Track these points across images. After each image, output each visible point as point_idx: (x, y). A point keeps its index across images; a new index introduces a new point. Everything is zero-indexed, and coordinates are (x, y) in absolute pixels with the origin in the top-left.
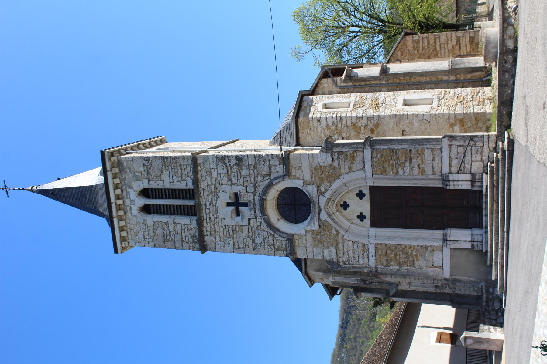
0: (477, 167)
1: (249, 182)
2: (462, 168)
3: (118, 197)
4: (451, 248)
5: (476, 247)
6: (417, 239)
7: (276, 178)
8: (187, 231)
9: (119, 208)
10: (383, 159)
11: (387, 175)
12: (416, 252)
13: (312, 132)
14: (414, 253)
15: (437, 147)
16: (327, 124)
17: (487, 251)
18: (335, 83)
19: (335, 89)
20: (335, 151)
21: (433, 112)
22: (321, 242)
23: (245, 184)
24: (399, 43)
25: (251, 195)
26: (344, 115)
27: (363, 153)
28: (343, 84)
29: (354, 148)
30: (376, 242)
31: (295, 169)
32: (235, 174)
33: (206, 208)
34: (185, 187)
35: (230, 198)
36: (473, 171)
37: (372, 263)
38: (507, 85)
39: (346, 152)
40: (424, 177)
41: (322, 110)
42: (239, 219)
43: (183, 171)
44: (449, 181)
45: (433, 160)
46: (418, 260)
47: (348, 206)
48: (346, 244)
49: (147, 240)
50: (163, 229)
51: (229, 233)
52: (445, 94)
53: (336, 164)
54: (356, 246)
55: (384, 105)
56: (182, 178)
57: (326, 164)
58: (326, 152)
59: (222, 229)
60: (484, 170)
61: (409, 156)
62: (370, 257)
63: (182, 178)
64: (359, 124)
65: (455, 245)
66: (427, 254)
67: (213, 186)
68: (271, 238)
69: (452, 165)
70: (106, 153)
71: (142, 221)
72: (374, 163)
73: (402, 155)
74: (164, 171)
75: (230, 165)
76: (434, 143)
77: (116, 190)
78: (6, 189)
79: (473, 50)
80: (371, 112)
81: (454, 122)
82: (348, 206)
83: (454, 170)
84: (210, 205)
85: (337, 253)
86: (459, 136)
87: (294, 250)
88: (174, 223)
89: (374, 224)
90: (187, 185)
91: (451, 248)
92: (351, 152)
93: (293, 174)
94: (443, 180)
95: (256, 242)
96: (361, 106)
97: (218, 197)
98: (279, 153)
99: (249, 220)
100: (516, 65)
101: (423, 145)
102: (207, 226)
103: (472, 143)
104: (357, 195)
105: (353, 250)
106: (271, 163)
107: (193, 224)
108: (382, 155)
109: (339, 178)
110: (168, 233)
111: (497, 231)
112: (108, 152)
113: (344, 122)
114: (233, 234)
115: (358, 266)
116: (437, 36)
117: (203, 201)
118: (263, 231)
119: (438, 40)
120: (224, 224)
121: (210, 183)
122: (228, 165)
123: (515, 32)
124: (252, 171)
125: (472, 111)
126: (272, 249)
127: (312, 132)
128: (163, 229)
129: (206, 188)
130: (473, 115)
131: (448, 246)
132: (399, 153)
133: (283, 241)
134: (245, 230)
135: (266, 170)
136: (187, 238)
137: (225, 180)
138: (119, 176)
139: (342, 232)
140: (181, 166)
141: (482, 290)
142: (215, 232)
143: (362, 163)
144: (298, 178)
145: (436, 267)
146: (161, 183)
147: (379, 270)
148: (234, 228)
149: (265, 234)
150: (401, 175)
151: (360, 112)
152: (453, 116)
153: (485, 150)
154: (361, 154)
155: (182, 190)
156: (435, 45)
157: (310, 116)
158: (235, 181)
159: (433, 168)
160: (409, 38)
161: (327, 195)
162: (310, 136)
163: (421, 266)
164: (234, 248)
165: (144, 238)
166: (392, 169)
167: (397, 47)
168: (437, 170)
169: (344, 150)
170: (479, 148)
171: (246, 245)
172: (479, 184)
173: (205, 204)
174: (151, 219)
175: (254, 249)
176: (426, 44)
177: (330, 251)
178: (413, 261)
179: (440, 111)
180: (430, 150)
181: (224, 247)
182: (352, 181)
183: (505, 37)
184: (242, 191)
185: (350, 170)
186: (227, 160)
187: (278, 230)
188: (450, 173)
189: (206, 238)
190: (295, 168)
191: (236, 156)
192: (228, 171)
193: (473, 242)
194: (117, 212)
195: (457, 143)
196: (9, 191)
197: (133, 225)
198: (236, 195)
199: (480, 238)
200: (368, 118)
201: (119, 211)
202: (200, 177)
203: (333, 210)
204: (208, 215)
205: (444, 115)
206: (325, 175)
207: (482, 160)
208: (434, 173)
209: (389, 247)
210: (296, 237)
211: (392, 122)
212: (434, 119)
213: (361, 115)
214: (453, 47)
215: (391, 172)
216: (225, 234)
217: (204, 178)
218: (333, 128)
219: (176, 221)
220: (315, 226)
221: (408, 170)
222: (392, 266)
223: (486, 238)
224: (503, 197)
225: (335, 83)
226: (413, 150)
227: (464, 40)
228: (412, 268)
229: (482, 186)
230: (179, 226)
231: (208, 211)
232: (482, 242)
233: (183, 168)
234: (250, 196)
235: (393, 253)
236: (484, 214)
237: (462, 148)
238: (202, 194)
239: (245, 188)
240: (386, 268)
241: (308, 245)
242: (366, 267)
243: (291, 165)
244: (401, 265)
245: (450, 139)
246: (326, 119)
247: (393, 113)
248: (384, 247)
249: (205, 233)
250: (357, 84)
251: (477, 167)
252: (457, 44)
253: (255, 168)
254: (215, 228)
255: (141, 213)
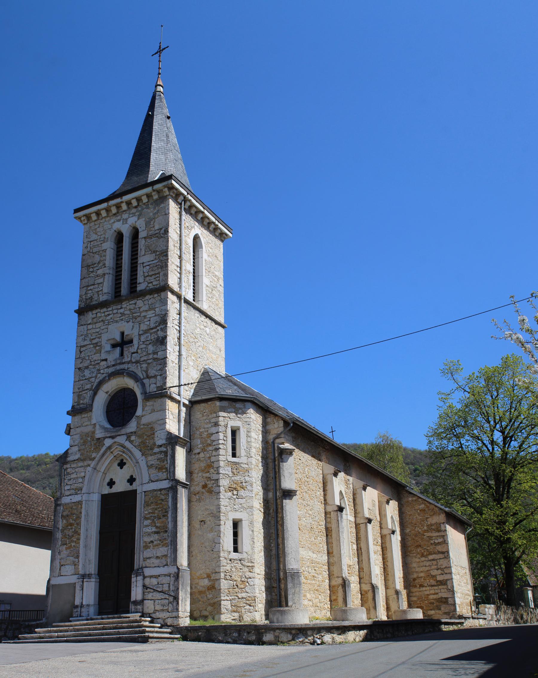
0: (149, 607)
1: (141, 355)
2: (149, 590)
3: (129, 203)
4: (75, 583)
5: (75, 610)
6: (86, 546)
7: (143, 385)
8: (97, 290)
9: (118, 206)
10: (159, 502)
11: (144, 507)
12: (74, 546)
13: (205, 418)
14: (73, 544)
15: (169, 560)
16: (212, 434)
17: (71, 621)
18: (278, 437)
19: (271, 437)
20: (168, 448)
21: (222, 554)
22: (85, 443)
23: (139, 351)
24: (436, 506)
25: (129, 359)
26: (222, 452)
27: (165, 480)
28: (276, 445)
29: (170, 469)
30: (84, 502)
31: (153, 405)
32: (150, 337)
33: (118, 309)
34: (138, 282)
35: (127, 335)
36: (145, 602)
37: (65, 500)
38: (226, 635)
39: (167, 460)
40: (142, 549)
41: (229, 426)
42: (108, 347)
43: (153, 277)
44: (136, 576)
45: (157, 557)
46: (66, 549)
47: (121, 468)
48: (82, 468)
49: (89, 245)
50: (99, 263)
51: (95, 339)
52: (248, 567)
53: (156, 450)
54: (80, 480)
55: (235, 497)
56: (147, 276)
57: (156, 439)
58: (167, 438)
59: (98, 330)
60: (146, 614)
61: (161, 530)
62: (70, 497)
63: (147, 276)
64: (212, 470)
65: (78, 588)
66: (72, 558)
67: (139, 314)
68: (89, 386)
69: (152, 579)
70: (169, 182)
71: (106, 237)
72: (155, 493)
73: (162, 522)
74: (154, 254)
75: (158, 330)
76: (173, 557)
77: (135, 200)
78: (160, 51)
79: (431, 603)
80: (224, 483)
81: (212, 578)
82: (121, 468)
83: (147, 581)
84: (121, 313)
85: (75, 460)
86: (178, 584)
87: (78, 413)
88: (104, 274)
89: (105, 498)
90: (140, 283)
91: (75, 583)
92: (166, 466)
93: (148, 404)
94: (138, 570)
95: (86, 371)
96: (234, 471)
97: (128, 322)
98: (168, 385)
99: (106, 360)
100: (245, 644)
101: (171, 545)
102: (101, 313)
103: (171, 599)
104: (132, 476)
105: (77, 478)
106: (159, 377)
107: (103, 297)
108: (162, 500)
109: (142, 455)
110: (95, 269)
111: (78, 630)
112: (172, 184)
113: (214, 453)
114: (93, 344)
115: (63, 485)
116: (446, 554)
117: (124, 305)
118: (96, 377)
119: (441, 556)
120: (102, 332)
121: (141, 310)
122: (158, 328)
123: (283, 643)
124: (151, 356)
125: (222, 598)
126: (79, 389)
127: (205, 418)
128: (99, 263)
129: (137, 307)
130: (219, 599)
131: (78, 581)
132: (164, 519)
133: (87, 400)
134: (96, 357)
135: (152, 372)
136: (90, 292)
137: (144, 327)
138: (151, 201)
139: (93, 464)
140: (159, 273)
141: (39, 620)
142: (96, 323)
143: (156, 478)
144: (143, 410)
145: (60, 570)
146: (143, 253)
147: (58, 508)
148: (99, 344)
149: (93, 380)
150: (143, 523)
151: (225, 470)
152: (217, 578)
153: (165, 614)
154: (165, 477)
155: (136, 279)
156: (435, 553)
157: (222, 414)
158: (143, 338)
159: (149, 558)
160: (442, 518)
161: (128, 444)
162: (201, 415)
163: (62, 553)
164: (81, 347)
165: (91, 242)
166: (149, 513)
167: (430, 503)
168: (148, 562)
169: (168, 458)
170: (167, 608)
171: (83, 359)
172: (133, 610)
173: (121, 308)
174: (109, 246)
175: (79, 369)
176: (436, 541)
177: (76, 454)
178: (66, 544)
179: (223, 562)
180: (166, 554)
181: (82, 335)
182: (140, 469)
183: (277, 631)
184: (133, 348)
185: (150, 467)
186: (162, 327)
187: (95, 394)
188: (144, 577)
189: (90, 313)
190: (153, 405)
191: (166, 337)
192: (152, 329)
193: (81, 607)
194: (114, 205)
195: (172, 583)
196: (157, 55)
197: (103, 227)
198: (131, 341)
199: (83, 614)
200: (217, 480)
201: (115, 207)
202: (148, 297)
203: (115, 451)
204: (111, 312)
205: (219, 566)
206: (146, 439)
207: (155, 611)
208: (145, 559)
209: (79, 517)
210: (89, 414)
211: (213, 508)
212: (215, 556)
213: (221, 472)
214: (434, 577)
215: (147, 512)
216: (94, 335)
217: (146, 302)
218: (209, 442)
219: (106, 276)
220: (99, 434)
221: (148, 530)
222: (62, 522)
223: (83, 620)
224: (102, 634)
225: (278, 437)
226: (166, 535)
227: (443, 591)
228: (60, 543)
229: (131, 613)
230: (101, 280)
231: (115, 311)
232: (80, 616)
233: (157, 276)
234: (128, 357)
235: (73, 522)
236: (103, 616)
237: (167, 589)
238: (131, 303)
239: (135, 351)
240: (60, 515)
241: (82, 429)
242: (61, 494)
243: (156, 400)
244: (62, 531)
245: (176, 575)
246: (217, 433)
247: (223, 509)
248: (79, 511)
249: (94, 312)
250: (277, 463)
251: (149, 607)
252: (437, 581)
253: (155, 359)
254: (100, 322)
255: (116, 234)
